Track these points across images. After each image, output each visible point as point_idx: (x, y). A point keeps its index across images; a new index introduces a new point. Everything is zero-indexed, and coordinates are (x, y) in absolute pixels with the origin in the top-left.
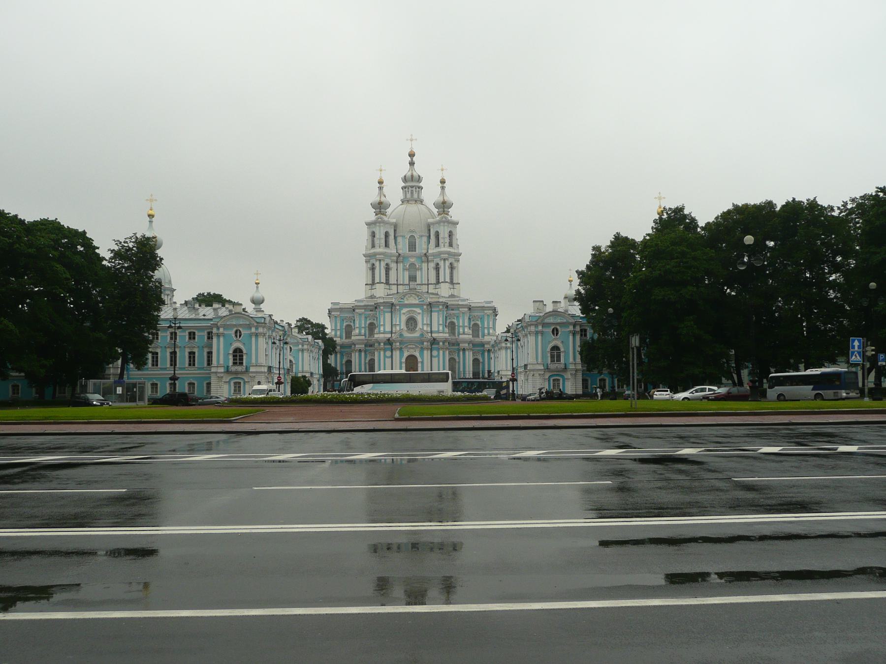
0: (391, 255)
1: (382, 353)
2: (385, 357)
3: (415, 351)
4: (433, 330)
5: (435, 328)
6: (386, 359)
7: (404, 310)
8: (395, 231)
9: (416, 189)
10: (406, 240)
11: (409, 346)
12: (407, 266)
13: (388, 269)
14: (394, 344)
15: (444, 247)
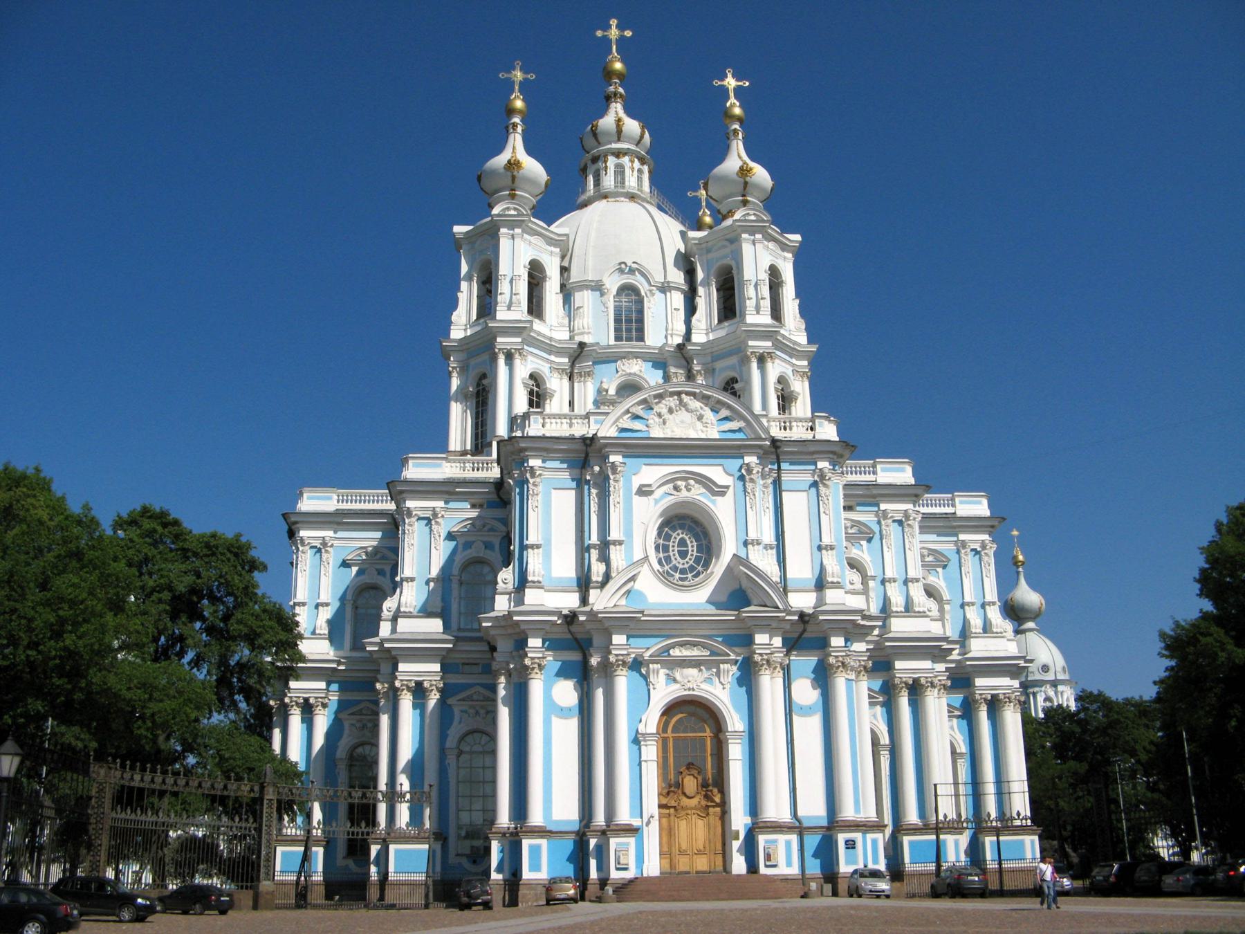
0: (549, 347)
1: (536, 687)
2: (552, 708)
3: (708, 680)
4: (789, 576)
5: (800, 568)
6: (554, 720)
7: (651, 473)
8: (564, 270)
9: (632, 162)
10: (604, 298)
11: (676, 652)
12: (612, 392)
13: (538, 396)
14: (597, 641)
15: (758, 313)
